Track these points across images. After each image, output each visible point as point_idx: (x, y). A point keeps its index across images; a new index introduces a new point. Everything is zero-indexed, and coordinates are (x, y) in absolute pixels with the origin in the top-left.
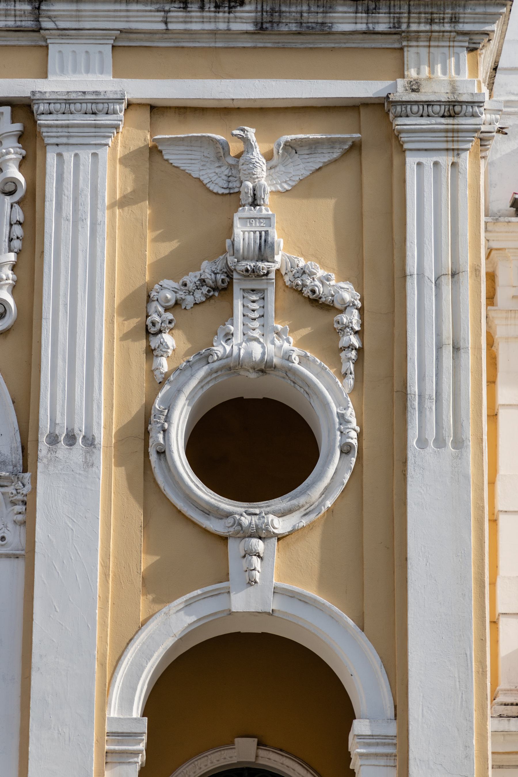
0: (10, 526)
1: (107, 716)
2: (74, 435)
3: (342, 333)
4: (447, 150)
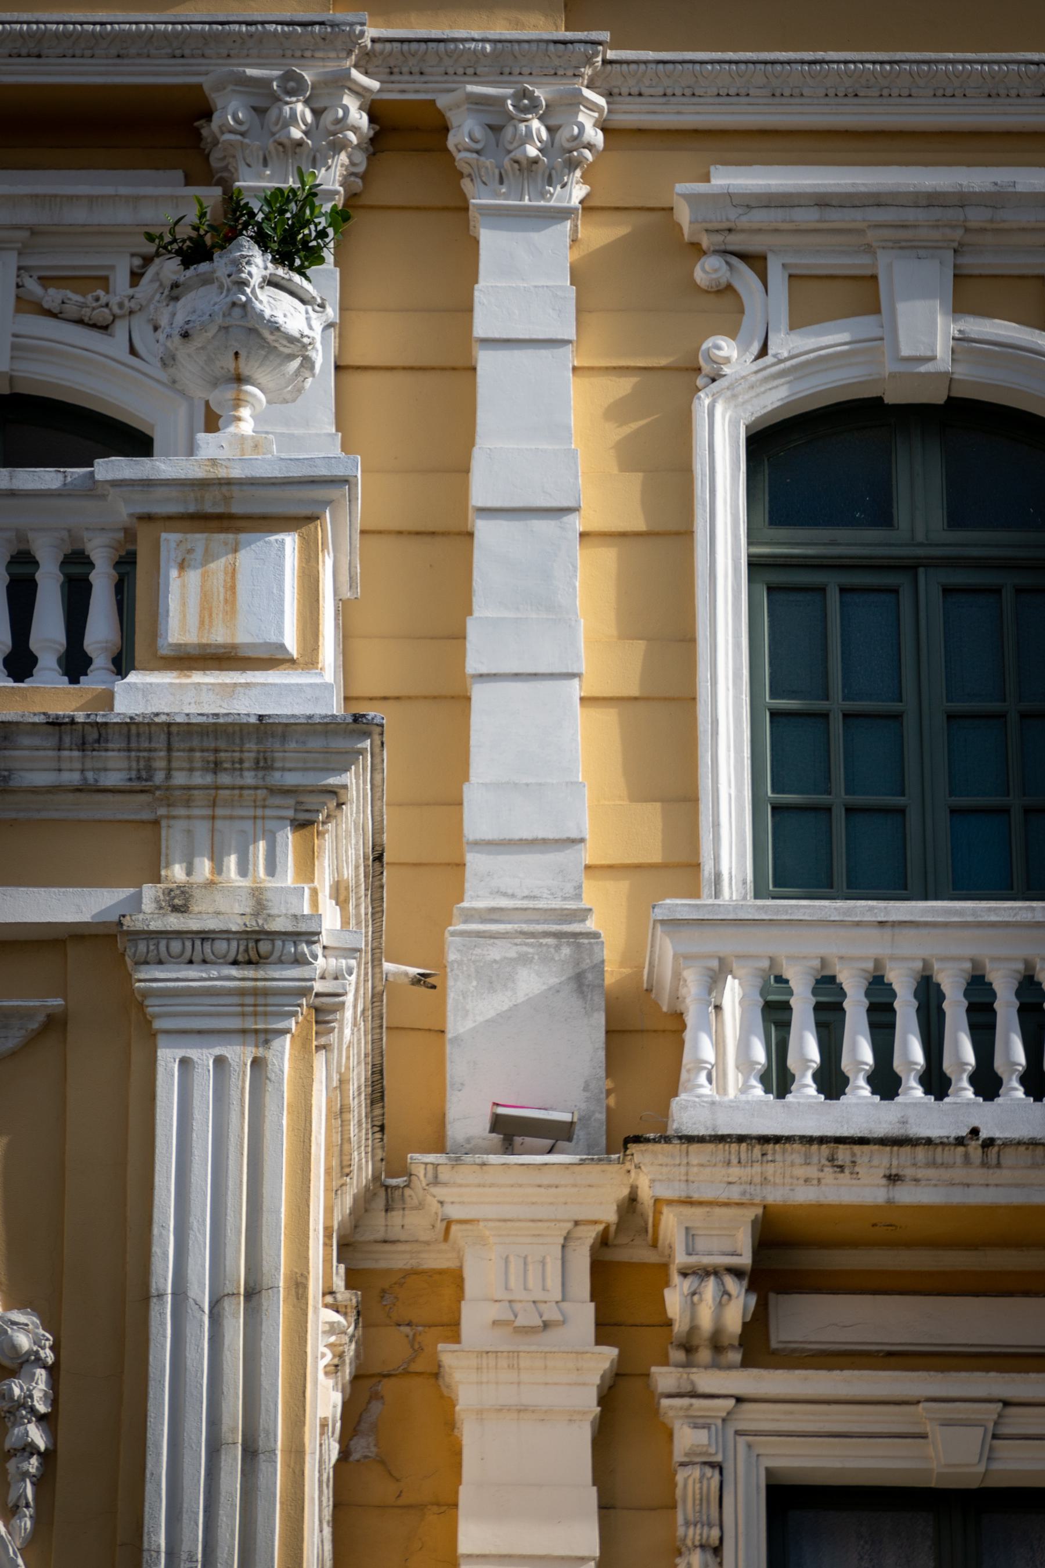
3: (12, 1418)
4: (244, 1032)
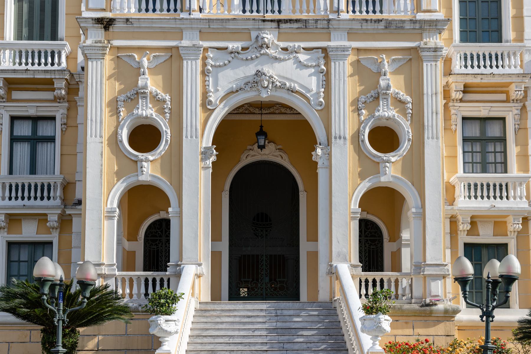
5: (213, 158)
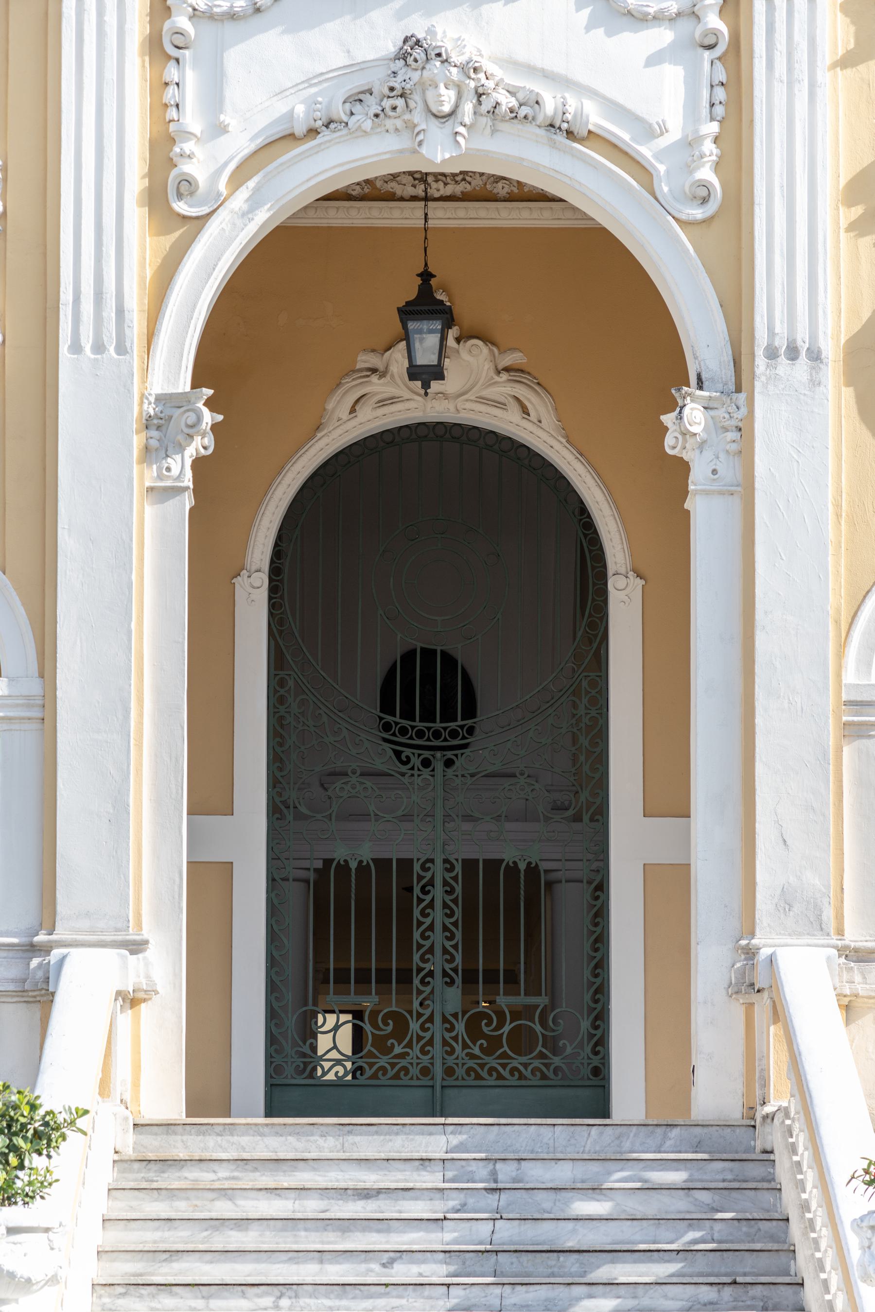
0: (722, 456)
1: (844, 682)
2: (796, 347)
5: (201, 444)
